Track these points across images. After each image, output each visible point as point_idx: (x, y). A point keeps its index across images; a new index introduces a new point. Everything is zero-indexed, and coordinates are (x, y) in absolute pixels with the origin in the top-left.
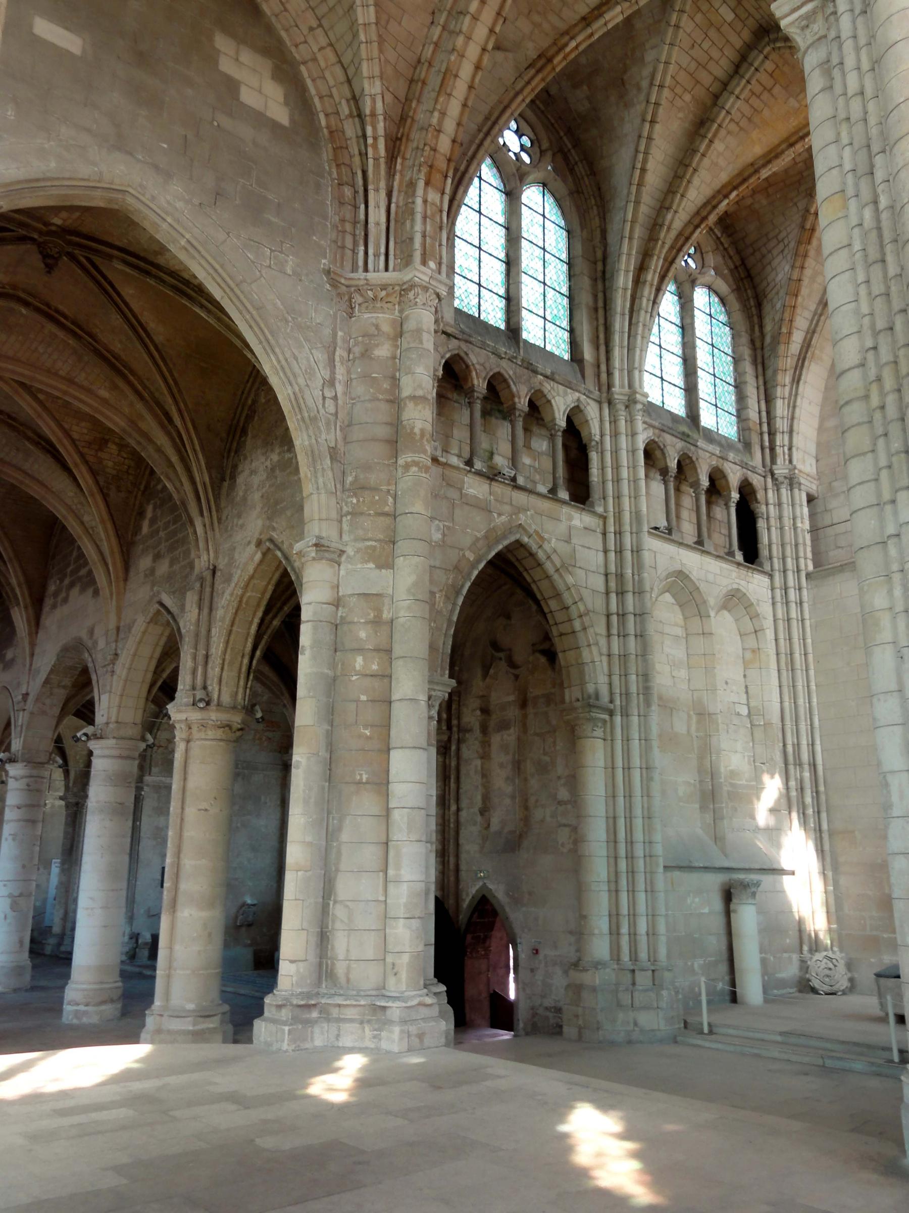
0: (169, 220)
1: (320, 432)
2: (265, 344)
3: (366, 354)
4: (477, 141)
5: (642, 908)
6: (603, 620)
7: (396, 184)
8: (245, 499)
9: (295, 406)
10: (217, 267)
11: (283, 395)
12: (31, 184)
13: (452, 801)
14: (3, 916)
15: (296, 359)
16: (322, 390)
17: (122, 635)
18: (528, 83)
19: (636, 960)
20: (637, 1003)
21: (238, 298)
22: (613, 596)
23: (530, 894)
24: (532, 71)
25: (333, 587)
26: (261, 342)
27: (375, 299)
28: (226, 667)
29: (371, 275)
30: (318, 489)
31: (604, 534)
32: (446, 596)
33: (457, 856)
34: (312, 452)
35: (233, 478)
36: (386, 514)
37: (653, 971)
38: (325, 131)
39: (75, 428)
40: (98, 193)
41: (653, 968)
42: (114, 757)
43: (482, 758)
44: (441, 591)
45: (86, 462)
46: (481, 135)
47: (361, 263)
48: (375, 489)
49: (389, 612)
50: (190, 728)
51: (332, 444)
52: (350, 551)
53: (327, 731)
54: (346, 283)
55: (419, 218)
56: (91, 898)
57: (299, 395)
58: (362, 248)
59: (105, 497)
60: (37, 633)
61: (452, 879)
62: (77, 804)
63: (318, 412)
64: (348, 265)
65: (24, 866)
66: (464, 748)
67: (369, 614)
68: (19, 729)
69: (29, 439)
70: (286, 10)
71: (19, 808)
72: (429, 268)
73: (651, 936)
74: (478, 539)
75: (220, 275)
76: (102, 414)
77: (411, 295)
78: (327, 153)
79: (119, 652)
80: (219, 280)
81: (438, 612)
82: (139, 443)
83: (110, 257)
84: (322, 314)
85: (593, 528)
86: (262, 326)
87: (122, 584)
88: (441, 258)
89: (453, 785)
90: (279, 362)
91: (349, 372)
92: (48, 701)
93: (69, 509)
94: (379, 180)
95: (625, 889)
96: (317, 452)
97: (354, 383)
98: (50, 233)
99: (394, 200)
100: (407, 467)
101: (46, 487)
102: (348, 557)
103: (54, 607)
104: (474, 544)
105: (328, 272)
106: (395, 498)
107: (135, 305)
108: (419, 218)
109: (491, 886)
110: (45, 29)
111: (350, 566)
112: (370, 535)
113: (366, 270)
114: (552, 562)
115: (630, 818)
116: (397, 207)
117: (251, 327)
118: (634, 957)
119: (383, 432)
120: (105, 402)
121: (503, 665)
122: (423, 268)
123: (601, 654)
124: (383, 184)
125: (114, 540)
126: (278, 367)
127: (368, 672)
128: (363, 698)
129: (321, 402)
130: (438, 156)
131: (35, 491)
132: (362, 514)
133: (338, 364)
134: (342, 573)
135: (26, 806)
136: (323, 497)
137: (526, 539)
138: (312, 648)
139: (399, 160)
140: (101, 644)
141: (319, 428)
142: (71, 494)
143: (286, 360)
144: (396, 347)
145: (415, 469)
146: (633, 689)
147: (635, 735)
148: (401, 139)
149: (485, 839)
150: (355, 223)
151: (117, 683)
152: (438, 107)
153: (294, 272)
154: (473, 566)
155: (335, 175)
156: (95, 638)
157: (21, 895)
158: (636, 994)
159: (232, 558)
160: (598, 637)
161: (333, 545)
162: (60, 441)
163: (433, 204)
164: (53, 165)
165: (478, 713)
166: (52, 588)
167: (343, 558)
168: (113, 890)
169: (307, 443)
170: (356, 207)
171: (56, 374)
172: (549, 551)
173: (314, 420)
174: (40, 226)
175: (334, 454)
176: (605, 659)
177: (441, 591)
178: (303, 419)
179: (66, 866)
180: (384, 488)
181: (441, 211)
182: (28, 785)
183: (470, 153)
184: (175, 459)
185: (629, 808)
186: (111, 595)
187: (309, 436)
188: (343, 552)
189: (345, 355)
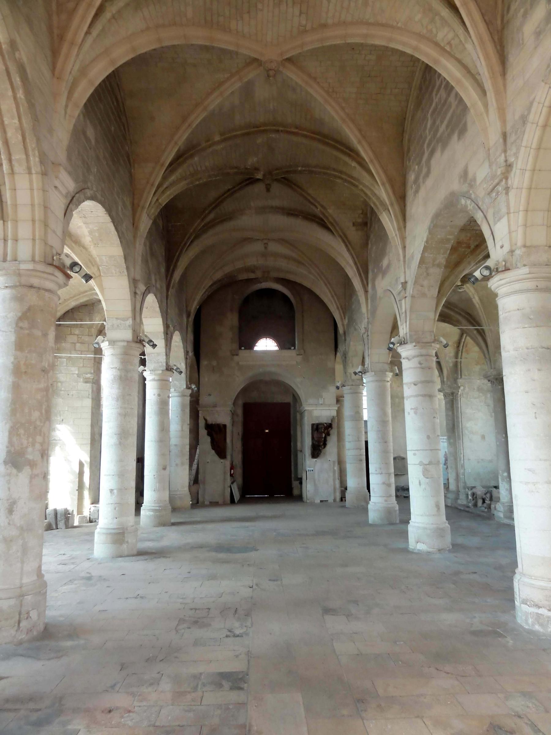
14: (418, 483)
17: (510, 140)
42: (528, 290)
56: (529, 470)
60: (405, 227)
62: (452, 394)
65: (428, 437)
68: (404, 315)
71: (415, 385)
79: (512, 159)
87: (500, 80)
92: (425, 283)
93: (420, 36)
101: (392, 27)
103: (417, 192)
131: (380, 38)
135: (422, 382)
142: (418, 17)
151: (517, 199)
156: (470, 175)
157: (430, 463)
166: (411, 177)
179: (452, 441)
182: (420, 363)
186: (486, 106)
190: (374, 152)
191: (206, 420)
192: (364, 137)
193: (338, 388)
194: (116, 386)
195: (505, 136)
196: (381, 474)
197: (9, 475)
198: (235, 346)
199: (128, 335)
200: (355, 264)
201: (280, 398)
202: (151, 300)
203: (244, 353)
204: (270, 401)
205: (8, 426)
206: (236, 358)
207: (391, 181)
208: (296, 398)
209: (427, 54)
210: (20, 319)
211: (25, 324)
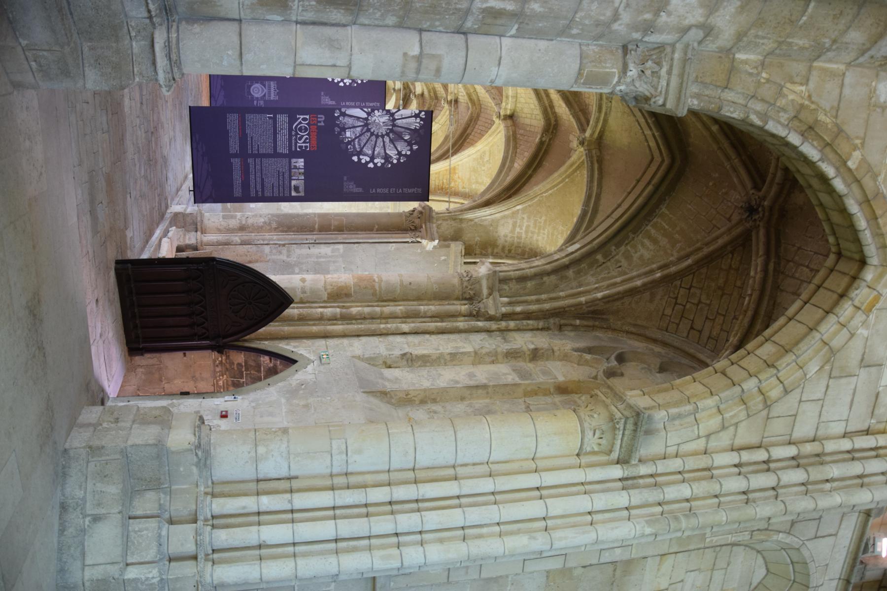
5: (307, 531)
6: (754, 440)
13: (413, 325)
19: (213, 527)
20: (135, 525)
22: (792, 451)
23: (307, 406)
31: (867, 432)
32: (802, 106)
33: (344, 335)
37: (195, 558)
41: (201, 556)
43: (476, 353)
44: (810, 96)
61: (315, 329)
66: (483, 336)
73: (257, 552)
74: (875, 177)
81: (782, 87)
85: (876, 412)
89: (432, 325)
95: (339, 502)
104: (870, 169)
109: (310, 368)
114: (835, 334)
115: (458, 501)
118: (218, 521)
121: (605, 365)
123: (708, 436)
137: (869, 275)
146: (671, 493)
147: (601, 501)
149: (371, 361)
154: (842, 164)
158: (153, 524)
160: (732, 429)
165: (532, 347)
172: (853, 323)
176: (700, 444)
177: (810, 96)
185: (476, 499)
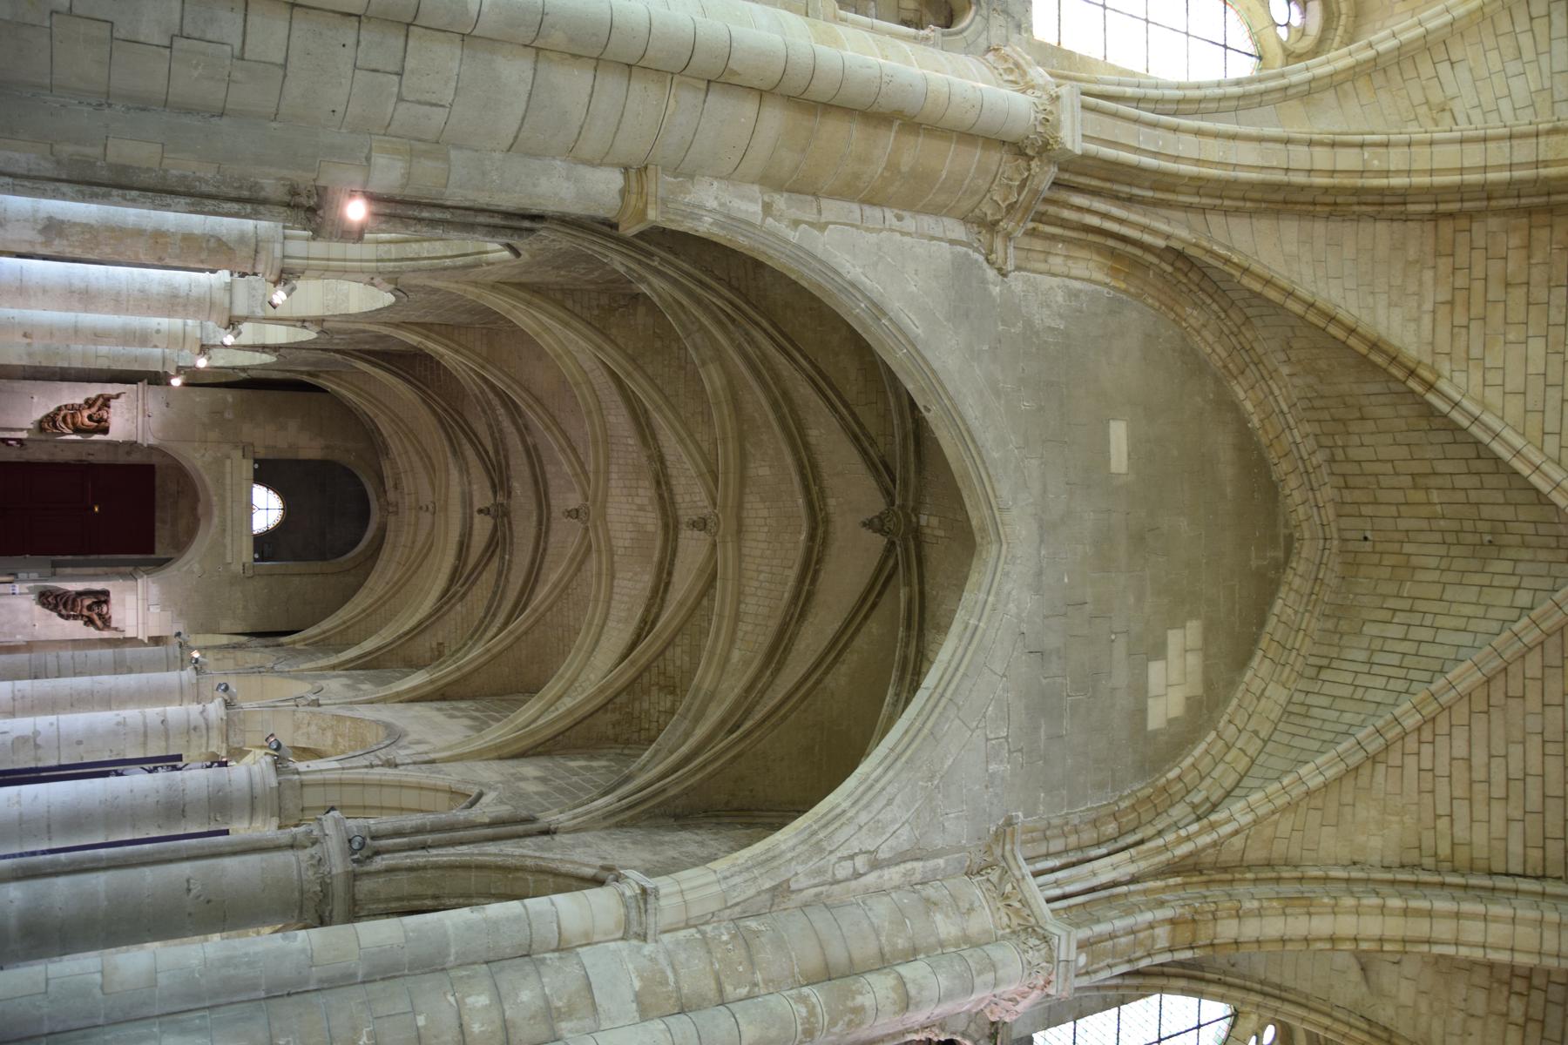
0: (991, 599)
1: (804, 862)
2: (893, 756)
3: (930, 904)
4: (1248, 984)
7: (1151, 884)
8: (662, 843)
9: (830, 816)
10: (962, 670)
11: (837, 798)
12: (966, 436)
15: (890, 802)
16: (861, 852)
18: (1351, 1026)
21: (935, 706)
24: (1364, 1026)
25: (586, 934)
26: (892, 750)
27: (1004, 897)
28: (413, 874)
29: (1030, 879)
30: (725, 878)
34: (774, 858)
35: (683, 827)
36: (721, 991)
38: (1163, 780)
39: (679, 650)
40: (987, 512)
45: (640, 675)
46: (1258, 987)
47: (1040, 866)
48: (752, 963)
49: (570, 1031)
50: (313, 844)
51: (794, 886)
52: (648, 948)
53: (353, 975)
54: (1008, 855)
55: (1128, 922)
57: (843, 819)
58: (1056, 862)
59: (603, 708)
63: (831, 852)
64: (1031, 850)
65: (79, 743)
67: (560, 999)
69: (648, 610)
70: (1259, 699)
72: (1078, 955)
75: (953, 676)
76: (709, 663)
77: (1033, 941)
78: (1142, 788)
80: (947, 677)
82: (688, 710)
83: (909, 584)
84: (956, 829)
86: (914, 746)
88: (1095, 972)
90: (877, 781)
91: (897, 888)
92: (313, 728)
94: (1145, 858)
96: (775, 864)
97: (886, 899)
98: (907, 516)
99: (1132, 887)
100: (803, 999)
102: (639, 949)
103: (439, 710)
105: (1010, 822)
106: (748, 997)
107: (859, 642)
108: (1128, 922)
110: (1119, 433)
111: (625, 953)
112: (682, 972)
113: (1036, 874)
116: (1126, 895)
117: (906, 732)
119: (837, 954)
120: (727, 659)
122: (1074, 946)
124: (1143, 865)
125: (548, 733)
126: (870, 781)
127: (466, 1018)
128: (421, 1021)
129: (845, 854)
130: (1210, 925)
132: (709, 952)
133: (902, 868)
134: (612, 945)
136: (716, 889)
138: (485, 920)
139: (1179, 880)
140: (403, 752)
141: (810, 858)
142: (592, 676)
143: (883, 789)
144: (957, 945)
145: (804, 1011)
148: (1201, 873)
150: (1080, 848)
152: (1265, 904)
153: (992, 776)
155: (1123, 805)
159: (574, 846)
161: (651, 919)
162: (658, 636)
163: (1153, 938)
164: (996, 455)
166: (463, 705)
167: (634, 942)
168: (49, 826)
169: (783, 847)
170: (1098, 844)
171: (739, 602)
173: (818, 848)
174: (911, 504)
175: (781, 891)
178: (814, 833)
180: (759, 977)
181: (1149, 955)
183: (1229, 979)
184: (684, 749)
187: (794, 848)
188: (645, 940)
189: (918, 877)
190: (501, 653)
191: (118, 396)
192: (518, 638)
193: (179, 634)
194: (162, 289)
195: (432, 762)
196: (14, 699)
197: (35, 221)
198: (262, 454)
199: (240, 310)
200: (379, 649)
201: (162, 534)
202: (308, 335)
203: (247, 467)
204: (158, 514)
205: (93, 222)
206: (240, 453)
207: (465, 678)
208: (162, 563)
209: (552, 689)
210: (219, 240)
211: (212, 244)
